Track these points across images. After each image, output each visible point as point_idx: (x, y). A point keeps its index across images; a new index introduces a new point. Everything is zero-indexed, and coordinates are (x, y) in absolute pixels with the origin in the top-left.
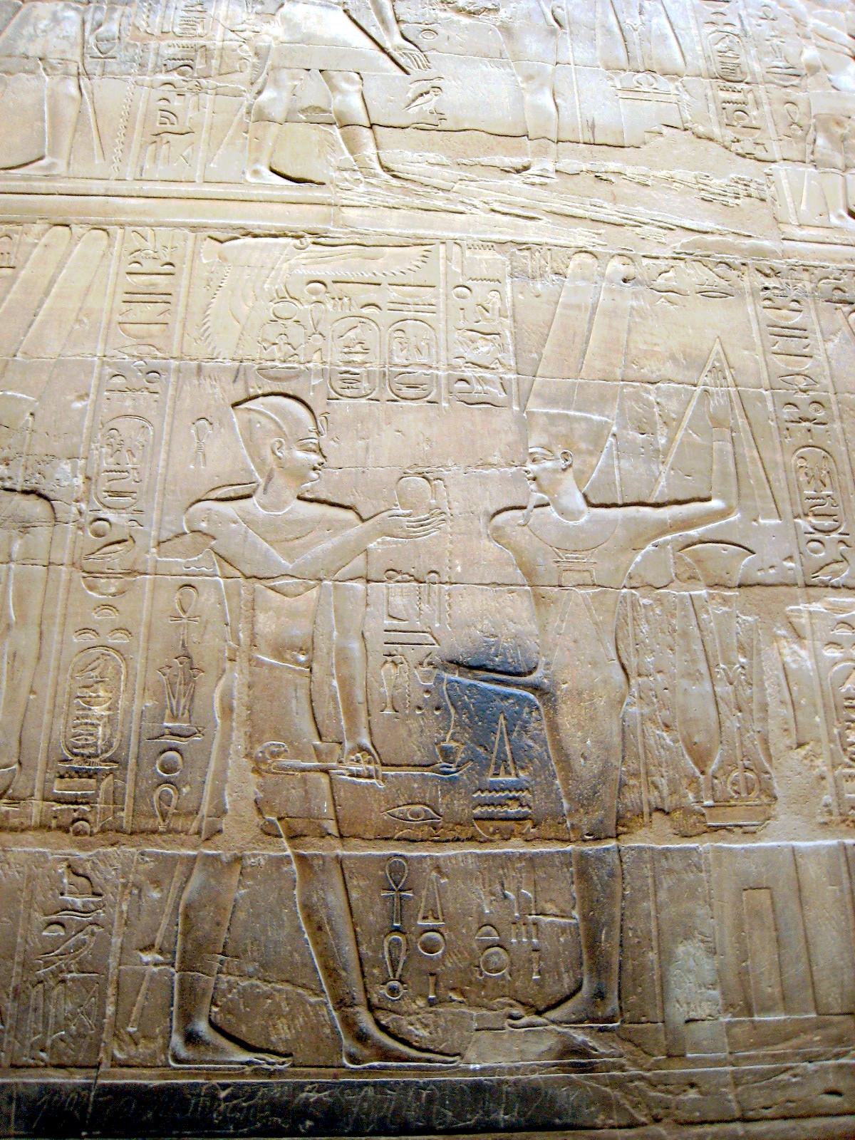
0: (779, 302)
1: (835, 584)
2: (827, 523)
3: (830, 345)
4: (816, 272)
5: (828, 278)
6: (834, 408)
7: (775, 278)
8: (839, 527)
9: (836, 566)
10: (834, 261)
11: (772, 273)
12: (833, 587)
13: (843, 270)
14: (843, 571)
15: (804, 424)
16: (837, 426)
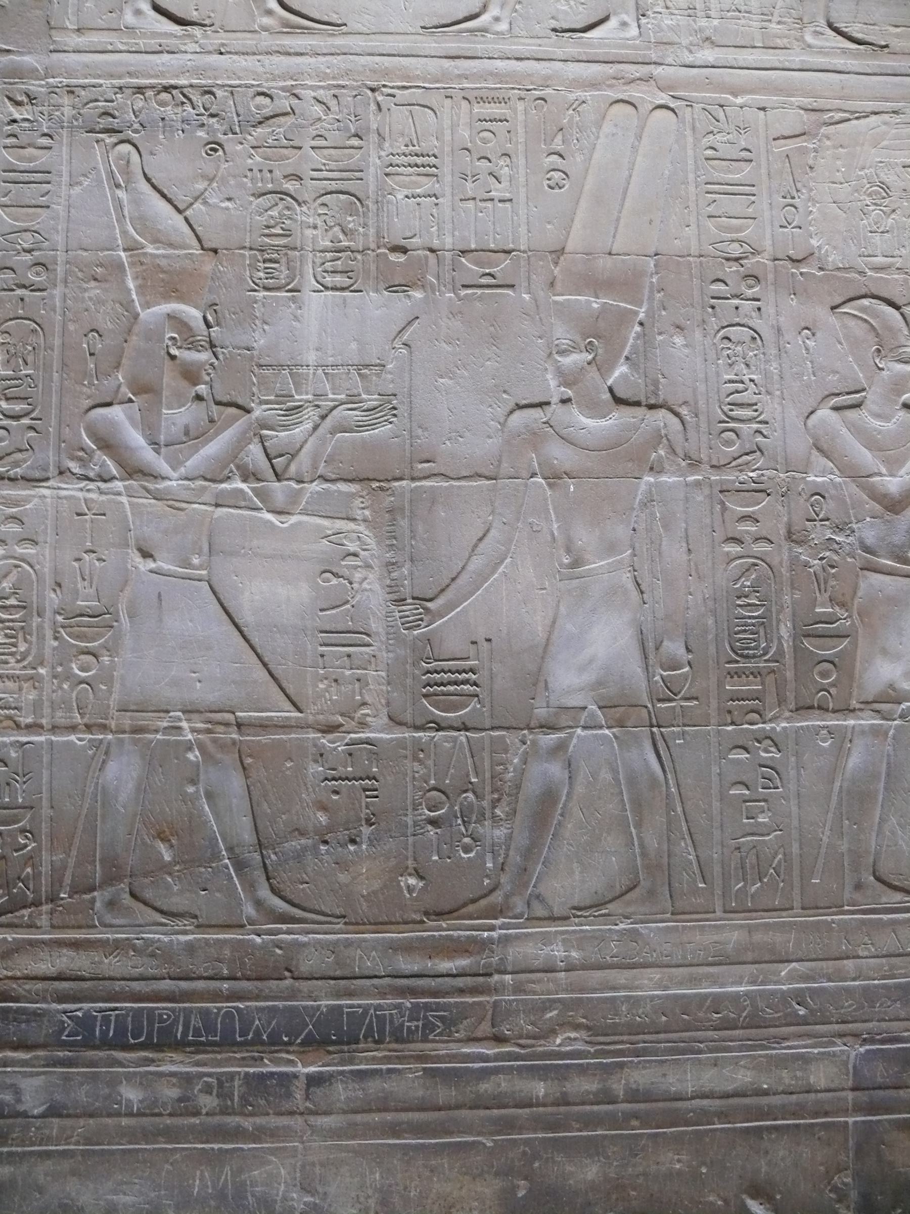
0: (24, 139)
1: (12, 477)
2: (18, 407)
3: (77, 190)
4: (83, 93)
5: (97, 100)
6: (60, 270)
7: (29, 107)
8: (33, 411)
9: (19, 456)
10: (112, 76)
11: (25, 100)
12: (10, 479)
13: (120, 88)
14: (25, 461)
15: (20, 292)
16: (57, 292)
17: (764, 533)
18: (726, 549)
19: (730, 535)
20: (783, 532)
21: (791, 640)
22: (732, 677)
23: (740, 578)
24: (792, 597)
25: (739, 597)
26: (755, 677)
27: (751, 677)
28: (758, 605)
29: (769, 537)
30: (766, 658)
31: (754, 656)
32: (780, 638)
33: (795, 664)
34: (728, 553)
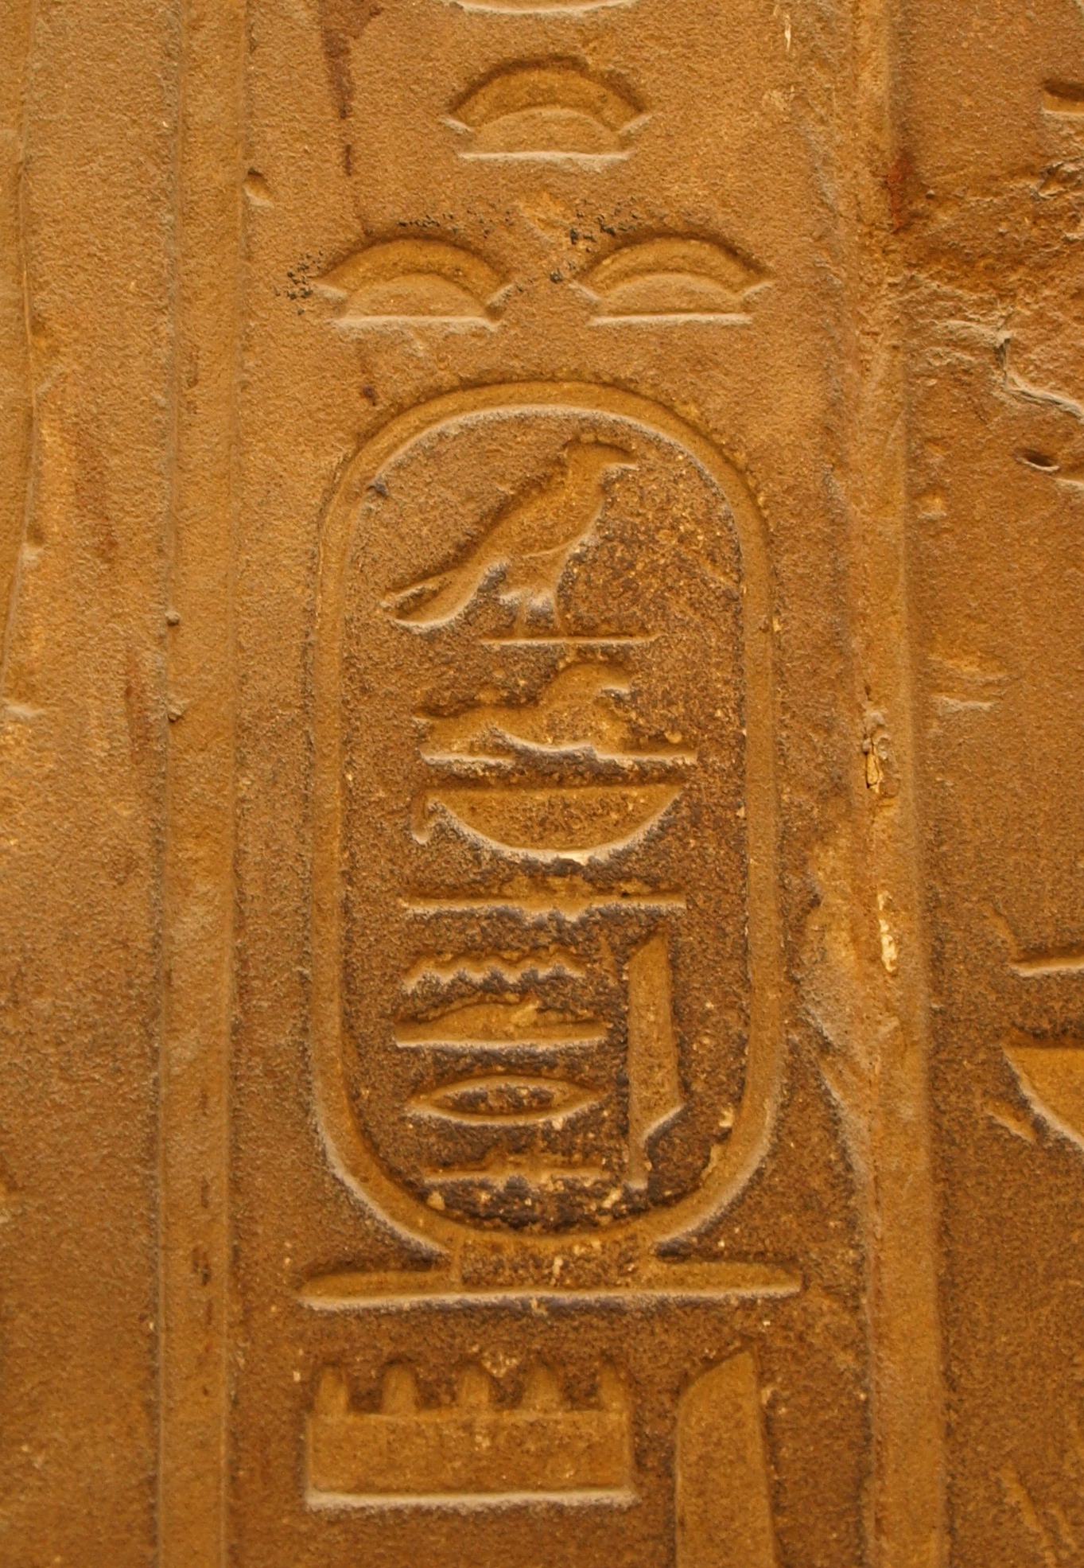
17: (685, 193)
18: (353, 322)
19: (388, 213)
20: (852, 187)
21: (911, 1072)
22: (366, 1400)
23: (465, 553)
24: (923, 713)
25: (449, 710)
26: (579, 1395)
27: (543, 1403)
28: (609, 776)
29: (720, 219)
30: (683, 1226)
31: (568, 1217)
32: (808, 1064)
33: (948, 1288)
34: (364, 351)
